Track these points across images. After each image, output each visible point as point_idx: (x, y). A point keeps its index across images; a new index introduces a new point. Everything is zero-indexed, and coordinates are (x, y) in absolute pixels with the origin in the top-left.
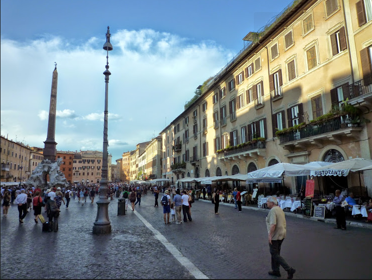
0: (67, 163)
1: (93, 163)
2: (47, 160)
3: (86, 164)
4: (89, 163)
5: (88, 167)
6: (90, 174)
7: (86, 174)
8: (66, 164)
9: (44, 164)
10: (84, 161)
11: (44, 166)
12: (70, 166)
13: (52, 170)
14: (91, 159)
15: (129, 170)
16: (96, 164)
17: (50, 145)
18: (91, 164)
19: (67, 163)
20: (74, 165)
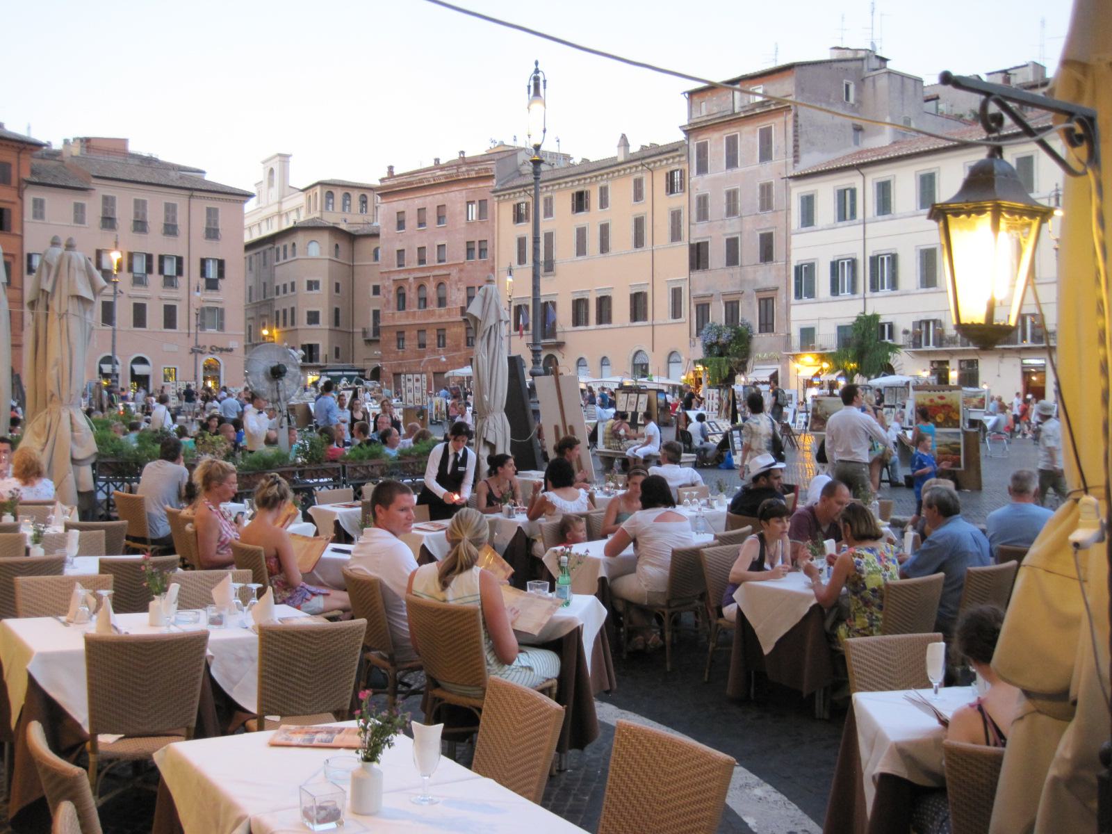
6: (155, 316)
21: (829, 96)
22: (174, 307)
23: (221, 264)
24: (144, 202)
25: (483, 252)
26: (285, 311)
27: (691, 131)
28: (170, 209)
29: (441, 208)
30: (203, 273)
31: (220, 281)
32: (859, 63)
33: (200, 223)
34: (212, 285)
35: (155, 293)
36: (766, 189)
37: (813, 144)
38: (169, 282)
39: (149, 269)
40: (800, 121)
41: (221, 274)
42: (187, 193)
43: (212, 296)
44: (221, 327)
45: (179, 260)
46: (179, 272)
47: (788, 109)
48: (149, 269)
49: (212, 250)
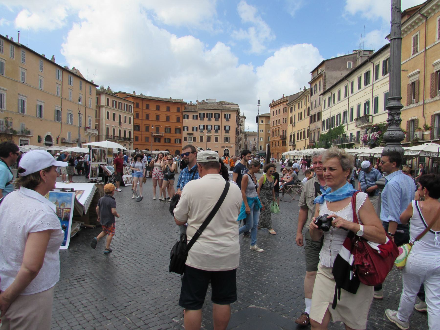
0: (173, 119)
1: (217, 120)
3: (206, 122)
4: (209, 120)
5: (209, 127)
6: (213, 139)
7: (205, 139)
8: (171, 121)
10: (202, 116)
12: (178, 125)
14: (213, 112)
15: (285, 132)
16: (222, 122)
18: (213, 122)
19: (173, 119)
20: (186, 123)
21: (340, 68)
23: (229, 127)
25: (286, 121)
26: (304, 138)
27: (311, 83)
29: (279, 110)
30: (225, 129)
34: (227, 132)
35: (205, 134)
36: (320, 98)
38: (216, 131)
41: (229, 129)
44: (229, 142)
45: (219, 126)
46: (219, 129)
47: (322, 75)
48: (212, 129)
49: (227, 124)
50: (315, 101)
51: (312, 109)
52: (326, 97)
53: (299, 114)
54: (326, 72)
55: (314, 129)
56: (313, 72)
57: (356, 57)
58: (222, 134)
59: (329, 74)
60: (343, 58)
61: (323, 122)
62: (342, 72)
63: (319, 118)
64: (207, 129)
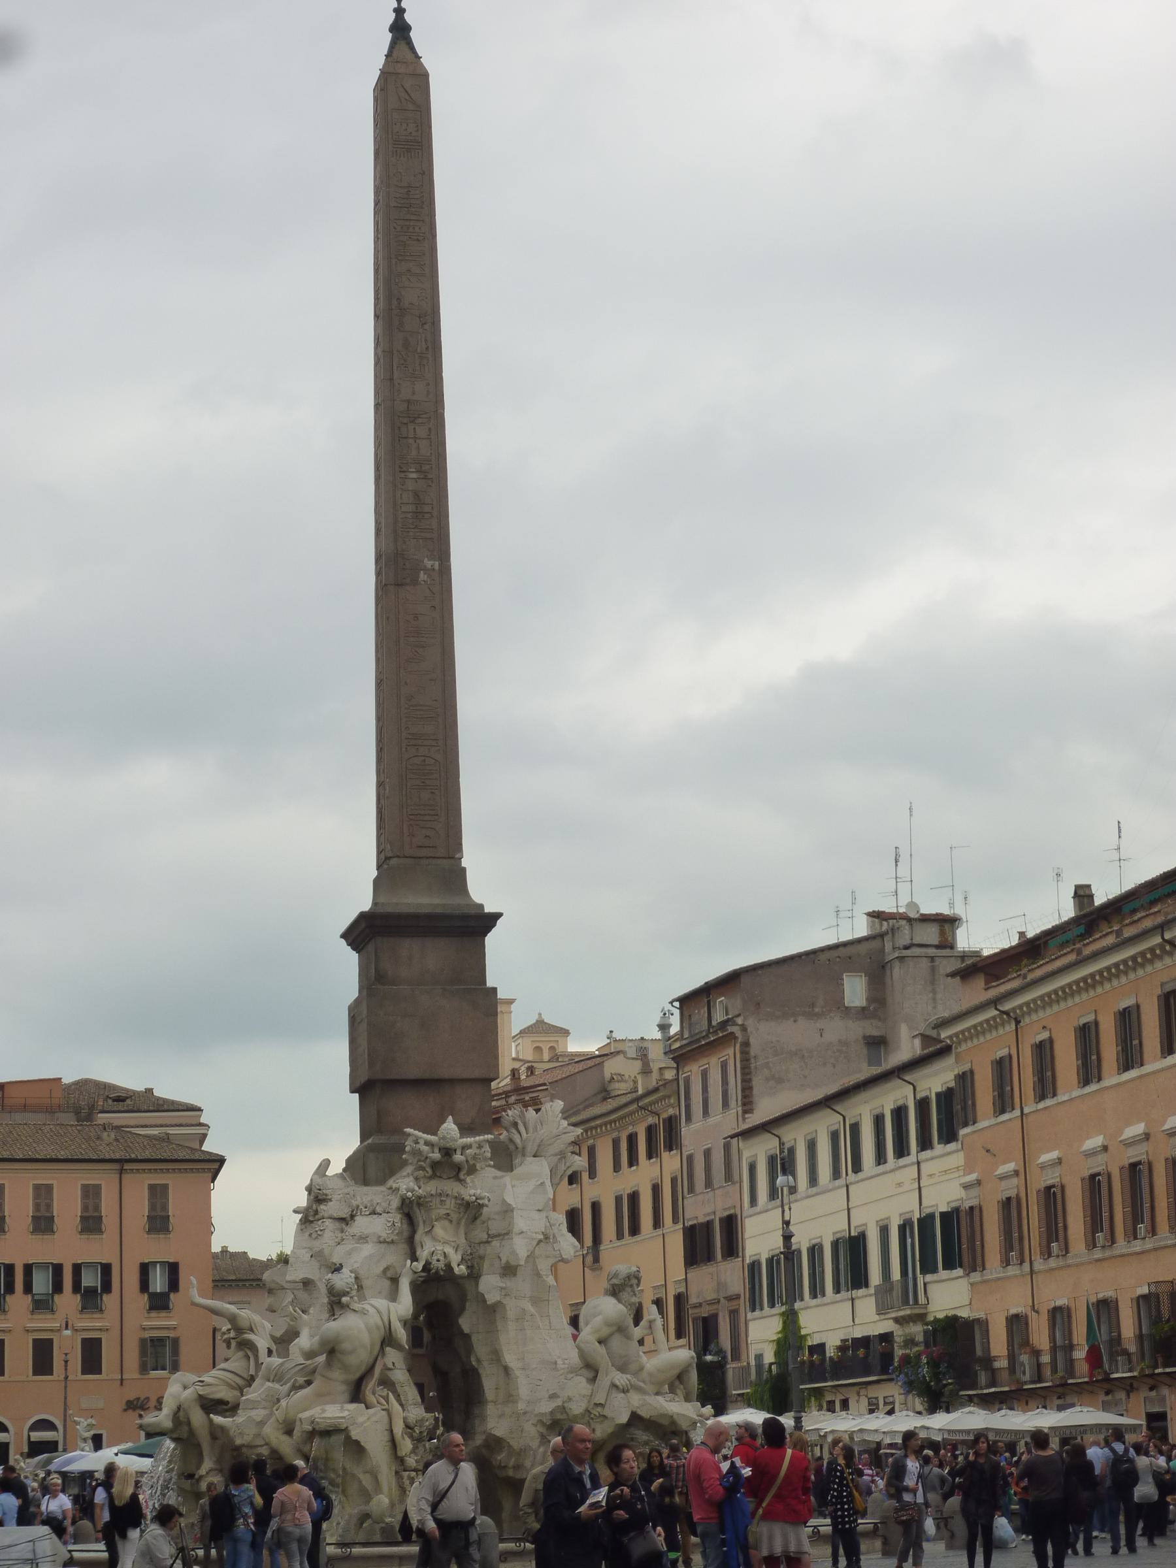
2: (450, 1127)
9: (405, 1183)
11: (409, 1211)
13: (520, 1248)
17: (425, 957)
21: (813, 1005)
22: (98, 1341)
23: (173, 1270)
24: (49, 1188)
28: (91, 1193)
30: (144, 1286)
31: (172, 1296)
32: (875, 944)
33: (138, 1206)
34: (159, 1303)
36: (727, 1148)
37: (780, 1081)
39: (58, 1287)
40: (753, 1051)
41: (174, 1285)
42: (116, 1166)
43: (160, 1320)
45: (106, 1269)
46: (107, 1287)
48: (58, 1287)
49: (159, 1250)
50: (707, 1153)
51: (691, 1189)
52: (760, 1150)
53: (618, 1199)
54: (750, 1023)
55: (711, 1296)
56: (687, 1001)
57: (882, 950)
58: (126, 1318)
59: (764, 1033)
60: (823, 957)
61: (754, 1267)
62: (820, 1024)
63: (732, 1248)
64: (28, 1288)
